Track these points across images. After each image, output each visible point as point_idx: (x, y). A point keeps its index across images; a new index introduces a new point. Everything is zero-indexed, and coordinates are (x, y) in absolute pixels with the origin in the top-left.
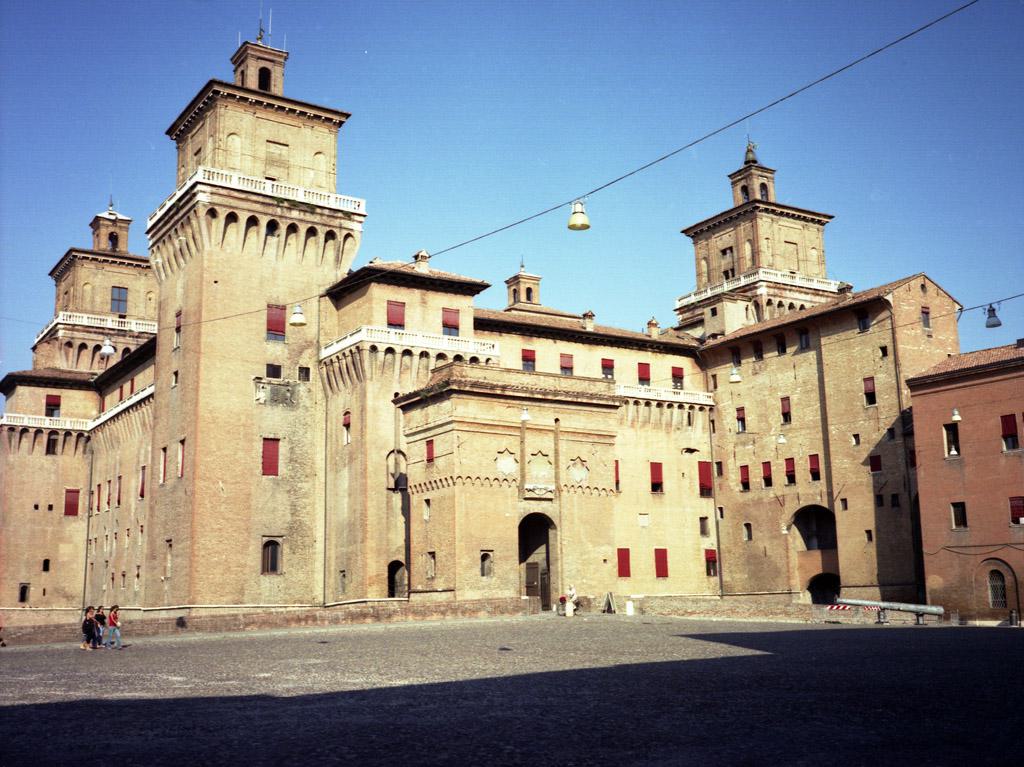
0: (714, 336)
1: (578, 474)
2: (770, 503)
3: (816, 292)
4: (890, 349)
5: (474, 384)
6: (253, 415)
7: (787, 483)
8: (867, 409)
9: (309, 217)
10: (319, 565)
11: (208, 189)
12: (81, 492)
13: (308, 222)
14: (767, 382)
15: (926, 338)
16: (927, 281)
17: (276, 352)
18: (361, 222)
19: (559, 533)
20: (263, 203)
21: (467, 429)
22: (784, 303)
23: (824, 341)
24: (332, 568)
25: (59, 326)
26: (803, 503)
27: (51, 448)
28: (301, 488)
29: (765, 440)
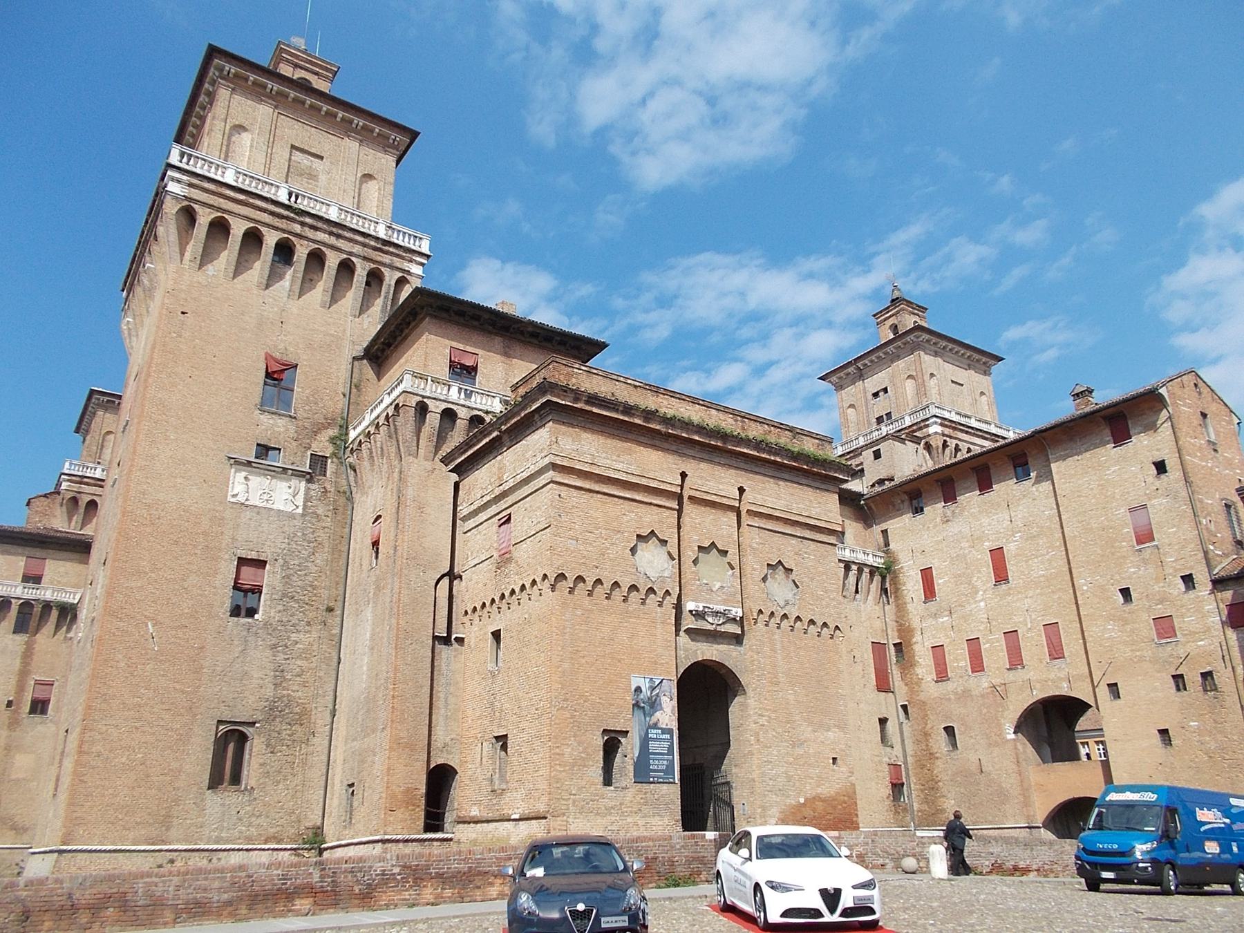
0: (881, 482)
1: (780, 589)
2: (982, 696)
3: (994, 437)
5: (593, 399)
6: (223, 518)
8: (1140, 550)
9: (341, 244)
10: (316, 775)
11: (185, 178)
12: (56, 684)
13: (340, 250)
15: (1213, 453)
16: (1199, 379)
17: (275, 427)
18: (422, 264)
19: (751, 702)
20: (272, 213)
21: (578, 483)
22: (961, 447)
23: (1053, 465)
24: (337, 781)
25: (63, 477)
26: (1039, 694)
27: (20, 627)
28: (297, 643)
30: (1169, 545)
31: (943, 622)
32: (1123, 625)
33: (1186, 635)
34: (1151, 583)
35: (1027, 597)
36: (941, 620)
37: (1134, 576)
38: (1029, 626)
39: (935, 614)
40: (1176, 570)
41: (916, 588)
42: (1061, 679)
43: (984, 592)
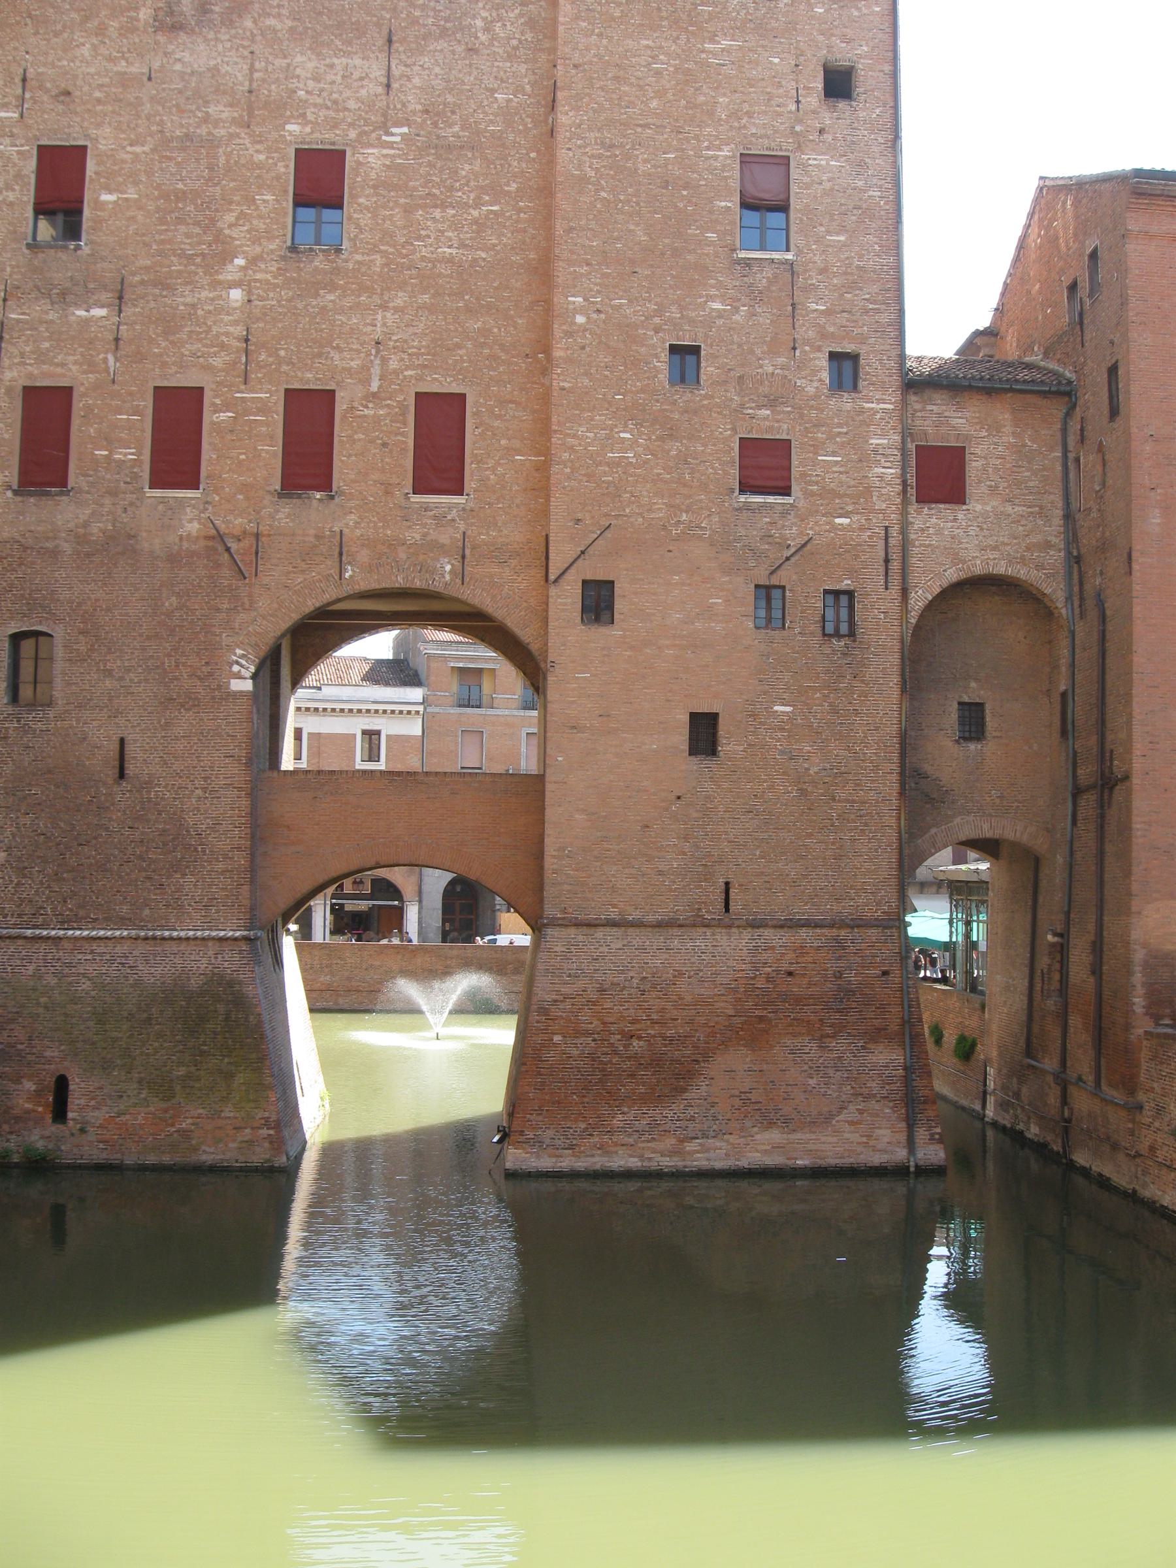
2: (173, 559)
4: (867, 80)
7: (278, 487)
8: (748, 263)
14: (236, 71)
29: (184, 297)
30: (823, 271)
31: (86, 322)
32: (661, 439)
33: (813, 494)
34: (758, 352)
35: (384, 307)
36: (81, 313)
37: (720, 322)
38: (375, 386)
39: (63, 294)
40: (824, 336)
41: (11, 196)
42: (442, 549)
43: (253, 261)
